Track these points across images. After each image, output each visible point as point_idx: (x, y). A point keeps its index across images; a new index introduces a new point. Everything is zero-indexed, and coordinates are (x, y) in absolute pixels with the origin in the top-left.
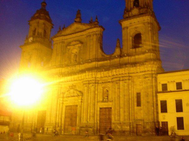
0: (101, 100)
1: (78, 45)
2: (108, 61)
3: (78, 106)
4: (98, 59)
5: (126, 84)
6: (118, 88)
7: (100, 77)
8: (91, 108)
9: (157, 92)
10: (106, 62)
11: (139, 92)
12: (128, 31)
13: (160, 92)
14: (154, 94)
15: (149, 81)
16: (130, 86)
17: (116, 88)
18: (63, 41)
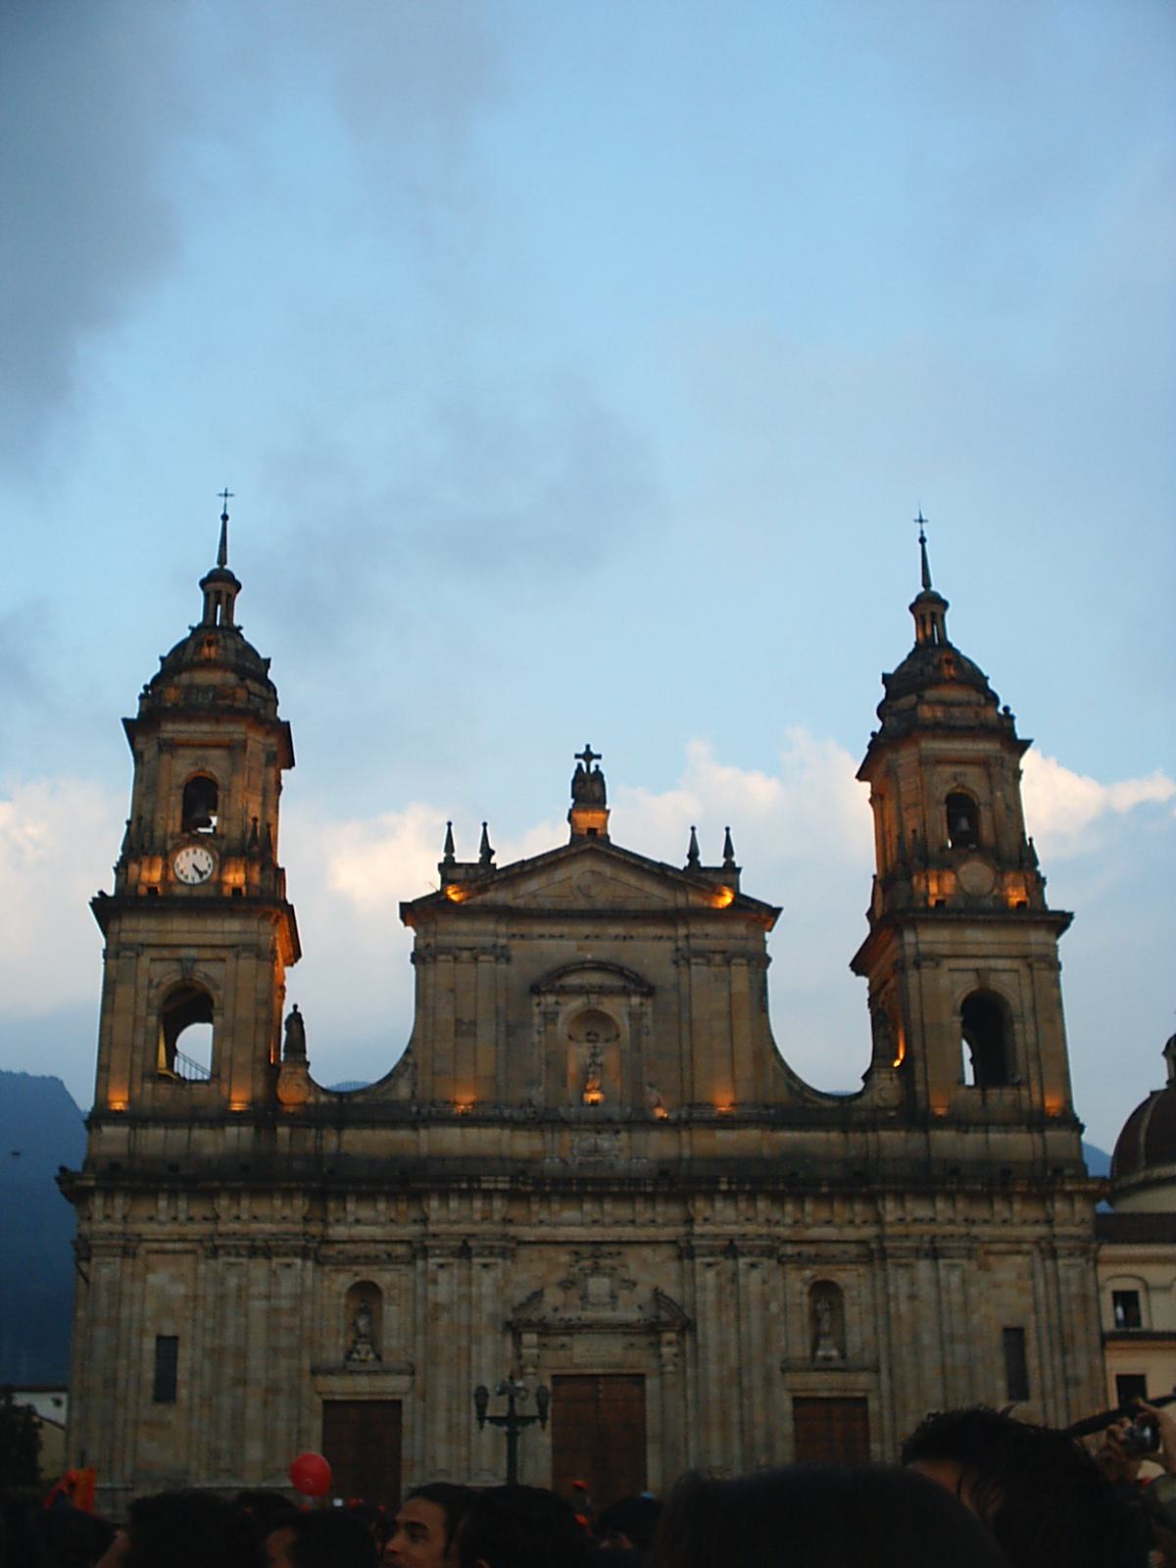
0: (800, 1349)
1: (621, 1000)
2: (834, 1136)
3: (652, 1384)
4: (767, 1107)
5: (955, 1279)
6: (913, 1297)
7: (789, 1220)
8: (758, 1398)
9: (1106, 1339)
10: (821, 1135)
11: (1015, 1325)
12: (944, 981)
13: (1113, 1337)
14: (1096, 1340)
15: (1073, 1274)
16: (973, 1291)
17: (902, 1298)
18: (502, 941)
